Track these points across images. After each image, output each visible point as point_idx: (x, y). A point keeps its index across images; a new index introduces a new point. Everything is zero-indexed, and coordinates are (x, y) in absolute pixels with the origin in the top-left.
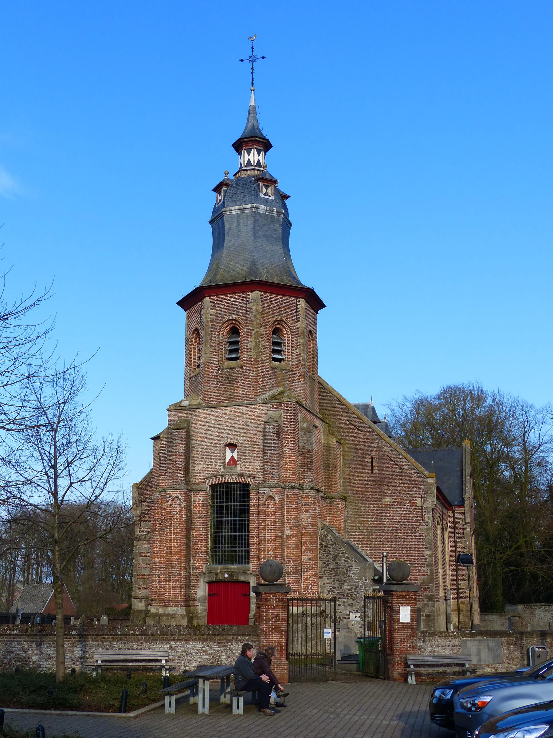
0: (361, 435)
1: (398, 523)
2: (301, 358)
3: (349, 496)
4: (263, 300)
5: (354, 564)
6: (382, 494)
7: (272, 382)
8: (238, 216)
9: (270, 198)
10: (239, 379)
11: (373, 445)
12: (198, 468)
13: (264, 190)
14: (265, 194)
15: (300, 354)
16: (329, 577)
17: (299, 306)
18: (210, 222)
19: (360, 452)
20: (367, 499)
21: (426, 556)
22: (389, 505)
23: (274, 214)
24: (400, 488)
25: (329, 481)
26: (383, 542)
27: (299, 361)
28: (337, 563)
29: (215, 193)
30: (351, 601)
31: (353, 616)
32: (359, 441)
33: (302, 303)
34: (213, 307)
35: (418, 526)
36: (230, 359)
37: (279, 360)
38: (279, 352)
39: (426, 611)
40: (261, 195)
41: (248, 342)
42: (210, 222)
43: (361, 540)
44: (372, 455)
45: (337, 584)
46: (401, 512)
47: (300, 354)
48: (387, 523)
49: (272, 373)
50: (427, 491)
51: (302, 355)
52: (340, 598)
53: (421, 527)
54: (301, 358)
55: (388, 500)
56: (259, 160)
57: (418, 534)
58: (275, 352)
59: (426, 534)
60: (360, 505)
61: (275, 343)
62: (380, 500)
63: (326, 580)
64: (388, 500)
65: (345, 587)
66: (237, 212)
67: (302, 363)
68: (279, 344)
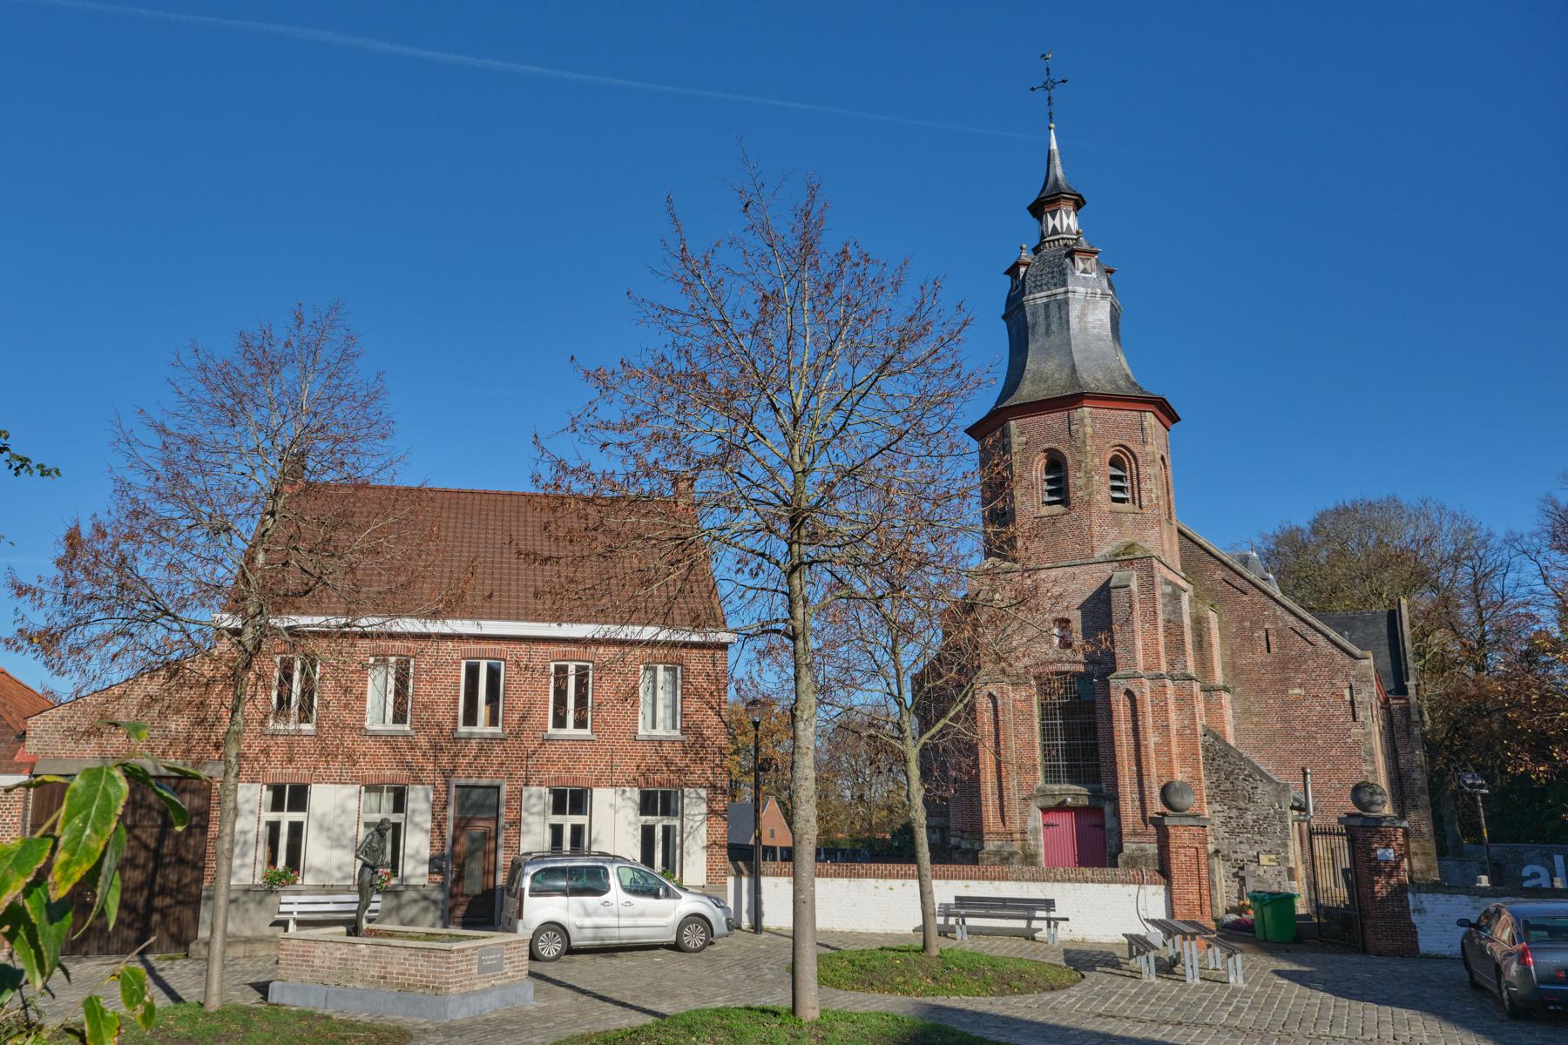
0: (1245, 598)
1: (1316, 724)
4: (1094, 419)
5: (1260, 785)
6: (1286, 683)
7: (1115, 531)
8: (1047, 305)
13: (1081, 266)
14: (1084, 271)
16: (1222, 802)
18: (1004, 317)
19: (1247, 624)
20: (1264, 691)
22: (1299, 700)
25: (1204, 663)
26: (1293, 752)
29: (1008, 278)
30: (1258, 837)
31: (1264, 859)
33: (1150, 419)
34: (1022, 433)
36: (1049, 503)
38: (1120, 489)
40: (1078, 273)
41: (1076, 479)
42: (1004, 317)
43: (1257, 749)
45: (1234, 813)
48: (1298, 724)
50: (1362, 679)
55: (1297, 691)
58: (1114, 488)
61: (1113, 477)
62: (1285, 692)
63: (1217, 807)
64: (1297, 691)
65: (1249, 817)
68: (1119, 478)
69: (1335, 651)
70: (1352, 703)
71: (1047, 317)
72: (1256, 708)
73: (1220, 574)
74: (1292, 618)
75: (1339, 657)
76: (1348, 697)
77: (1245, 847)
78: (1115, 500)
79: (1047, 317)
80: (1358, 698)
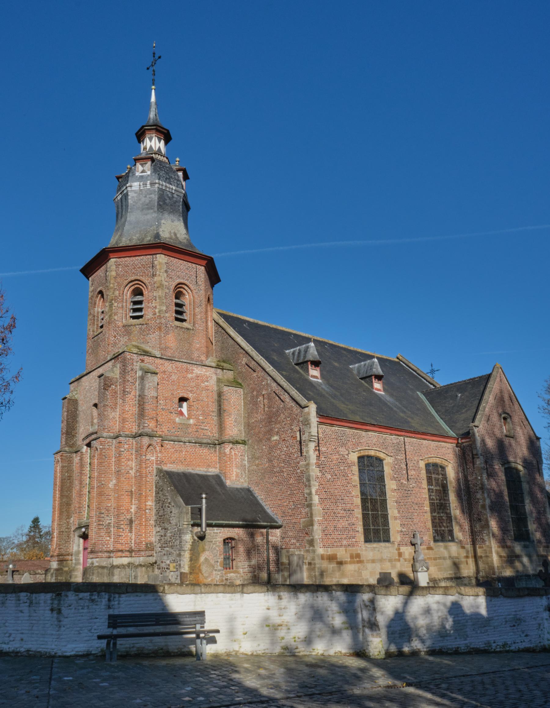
0: (255, 375)
2: (157, 311)
3: (248, 440)
6: (270, 432)
9: (145, 174)
10: (101, 343)
11: (263, 383)
12: (81, 430)
15: (156, 307)
17: (156, 262)
19: (255, 393)
21: (305, 495)
22: (277, 443)
23: (148, 186)
24: (284, 423)
27: (155, 314)
28: (164, 510)
32: (254, 382)
35: (298, 463)
37: (141, 317)
38: (140, 310)
39: (308, 558)
44: (263, 393)
46: (285, 449)
47: (156, 307)
49: (126, 330)
51: (158, 307)
52: (165, 547)
53: (301, 463)
54: (157, 311)
56: (159, 148)
57: (299, 471)
58: (135, 310)
59: (305, 470)
60: (256, 447)
61: (135, 303)
62: (269, 439)
66: (120, 196)
67: (158, 314)
68: (140, 302)
69: (293, 404)
70: (300, 443)
71: (122, 206)
72: (257, 455)
73: (244, 360)
74: (274, 385)
75: (296, 409)
76: (298, 439)
77: (165, 558)
78: (134, 318)
79: (122, 206)
80: (303, 438)
